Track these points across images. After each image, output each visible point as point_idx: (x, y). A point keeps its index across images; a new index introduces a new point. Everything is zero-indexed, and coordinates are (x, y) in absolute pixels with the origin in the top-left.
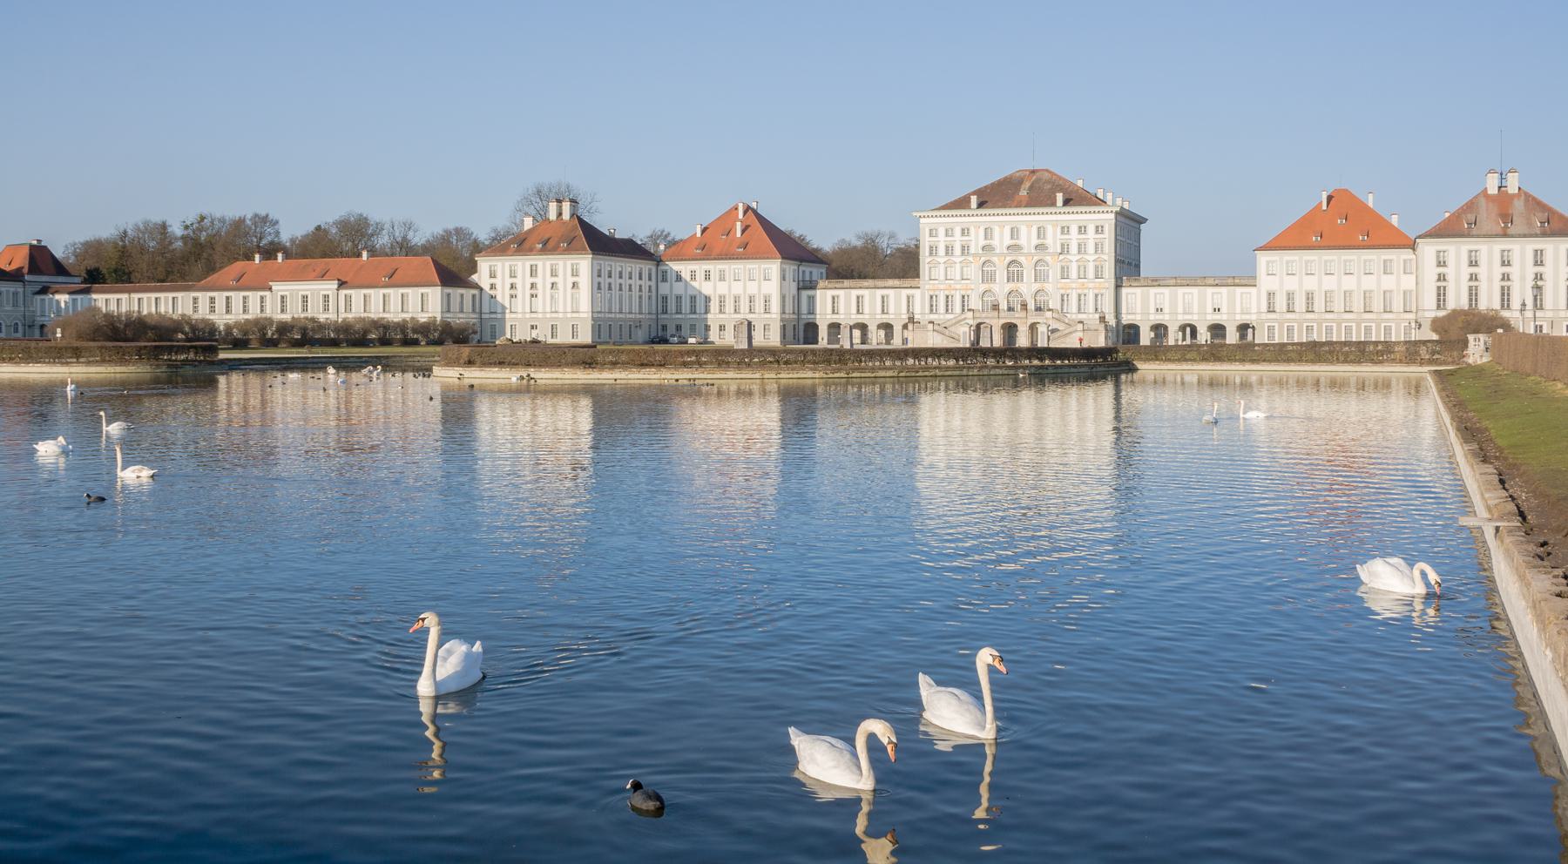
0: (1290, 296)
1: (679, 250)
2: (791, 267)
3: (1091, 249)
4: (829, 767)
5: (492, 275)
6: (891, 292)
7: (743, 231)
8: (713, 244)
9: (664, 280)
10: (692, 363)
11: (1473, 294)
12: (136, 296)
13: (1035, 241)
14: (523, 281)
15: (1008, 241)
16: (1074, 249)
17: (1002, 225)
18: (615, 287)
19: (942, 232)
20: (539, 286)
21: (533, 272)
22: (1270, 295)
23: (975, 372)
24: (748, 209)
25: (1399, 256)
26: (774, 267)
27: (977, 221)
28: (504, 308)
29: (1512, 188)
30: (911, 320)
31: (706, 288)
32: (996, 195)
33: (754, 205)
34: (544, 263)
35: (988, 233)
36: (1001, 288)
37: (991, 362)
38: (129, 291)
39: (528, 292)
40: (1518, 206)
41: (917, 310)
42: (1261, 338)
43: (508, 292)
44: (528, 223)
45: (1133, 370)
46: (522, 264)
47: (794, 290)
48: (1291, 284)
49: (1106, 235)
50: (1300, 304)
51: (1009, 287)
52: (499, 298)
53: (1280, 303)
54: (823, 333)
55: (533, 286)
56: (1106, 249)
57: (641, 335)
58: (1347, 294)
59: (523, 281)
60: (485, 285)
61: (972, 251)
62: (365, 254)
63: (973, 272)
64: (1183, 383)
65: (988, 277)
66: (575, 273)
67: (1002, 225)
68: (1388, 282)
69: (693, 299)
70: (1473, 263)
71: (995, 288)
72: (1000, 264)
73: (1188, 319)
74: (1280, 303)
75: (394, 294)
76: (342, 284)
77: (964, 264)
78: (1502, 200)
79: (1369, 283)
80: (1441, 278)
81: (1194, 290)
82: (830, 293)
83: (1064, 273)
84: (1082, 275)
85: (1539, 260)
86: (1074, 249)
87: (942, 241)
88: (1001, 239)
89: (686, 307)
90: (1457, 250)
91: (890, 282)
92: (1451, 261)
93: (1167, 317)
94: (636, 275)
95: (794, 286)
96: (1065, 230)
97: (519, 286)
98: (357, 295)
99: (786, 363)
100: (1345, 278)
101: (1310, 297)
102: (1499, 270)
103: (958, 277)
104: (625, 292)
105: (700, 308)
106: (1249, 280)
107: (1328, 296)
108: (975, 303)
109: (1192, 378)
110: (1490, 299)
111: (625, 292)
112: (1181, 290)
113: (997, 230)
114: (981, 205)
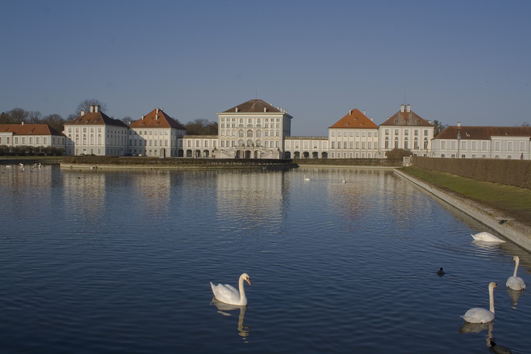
0: (339, 143)
1: (136, 124)
2: (175, 131)
3: (275, 126)
4: (477, 317)
5: (70, 132)
6: (208, 140)
7: (158, 118)
8: (148, 122)
9: (131, 134)
10: (154, 163)
11: (396, 144)
13: (257, 124)
14: (81, 134)
15: (248, 123)
16: (269, 126)
17: (246, 118)
18: (114, 136)
19: (226, 119)
20: (87, 136)
21: (85, 131)
22: (333, 143)
23: (249, 167)
24: (159, 110)
26: (168, 131)
27: (238, 116)
28: (74, 143)
29: (408, 111)
30: (215, 149)
31: (145, 137)
32: (244, 108)
33: (162, 109)
34: (89, 128)
35: (241, 120)
36: (245, 139)
37: (253, 164)
39: (83, 138)
40: (410, 116)
41: (217, 146)
42: (330, 157)
43: (75, 138)
44: (83, 113)
45: (298, 167)
46: (81, 128)
47: (175, 139)
48: (339, 139)
49: (280, 122)
50: (342, 146)
51: (248, 139)
52: (72, 140)
53: (336, 146)
54: (185, 153)
55: (84, 135)
56: (280, 126)
57: (122, 153)
58: (357, 143)
59: (81, 134)
60: (67, 135)
62: (23, 123)
63: (236, 133)
64: (313, 171)
65: (241, 135)
66: (100, 131)
67: (246, 118)
68: (370, 139)
69: (141, 141)
70: (397, 134)
71: (243, 139)
72: (245, 131)
73: (306, 150)
74: (336, 146)
75: (34, 137)
76: (14, 134)
78: (405, 114)
79: (364, 139)
80: (387, 138)
81: (308, 141)
82: (188, 140)
84: (272, 135)
86: (269, 126)
87: (226, 122)
88: (246, 123)
89: (138, 144)
90: (392, 130)
91: (208, 136)
92: (390, 133)
93: (299, 149)
94: (121, 132)
95: (175, 137)
96: (267, 120)
97: (79, 135)
98: (20, 138)
99: (186, 163)
100: (356, 138)
101: (345, 143)
102: (404, 136)
103: (231, 135)
104: (117, 138)
105: (143, 144)
106: (326, 138)
107: (351, 143)
108: (236, 144)
109: (316, 170)
110: (401, 145)
111: (117, 138)
112: (304, 141)
113: (244, 119)
114: (239, 111)
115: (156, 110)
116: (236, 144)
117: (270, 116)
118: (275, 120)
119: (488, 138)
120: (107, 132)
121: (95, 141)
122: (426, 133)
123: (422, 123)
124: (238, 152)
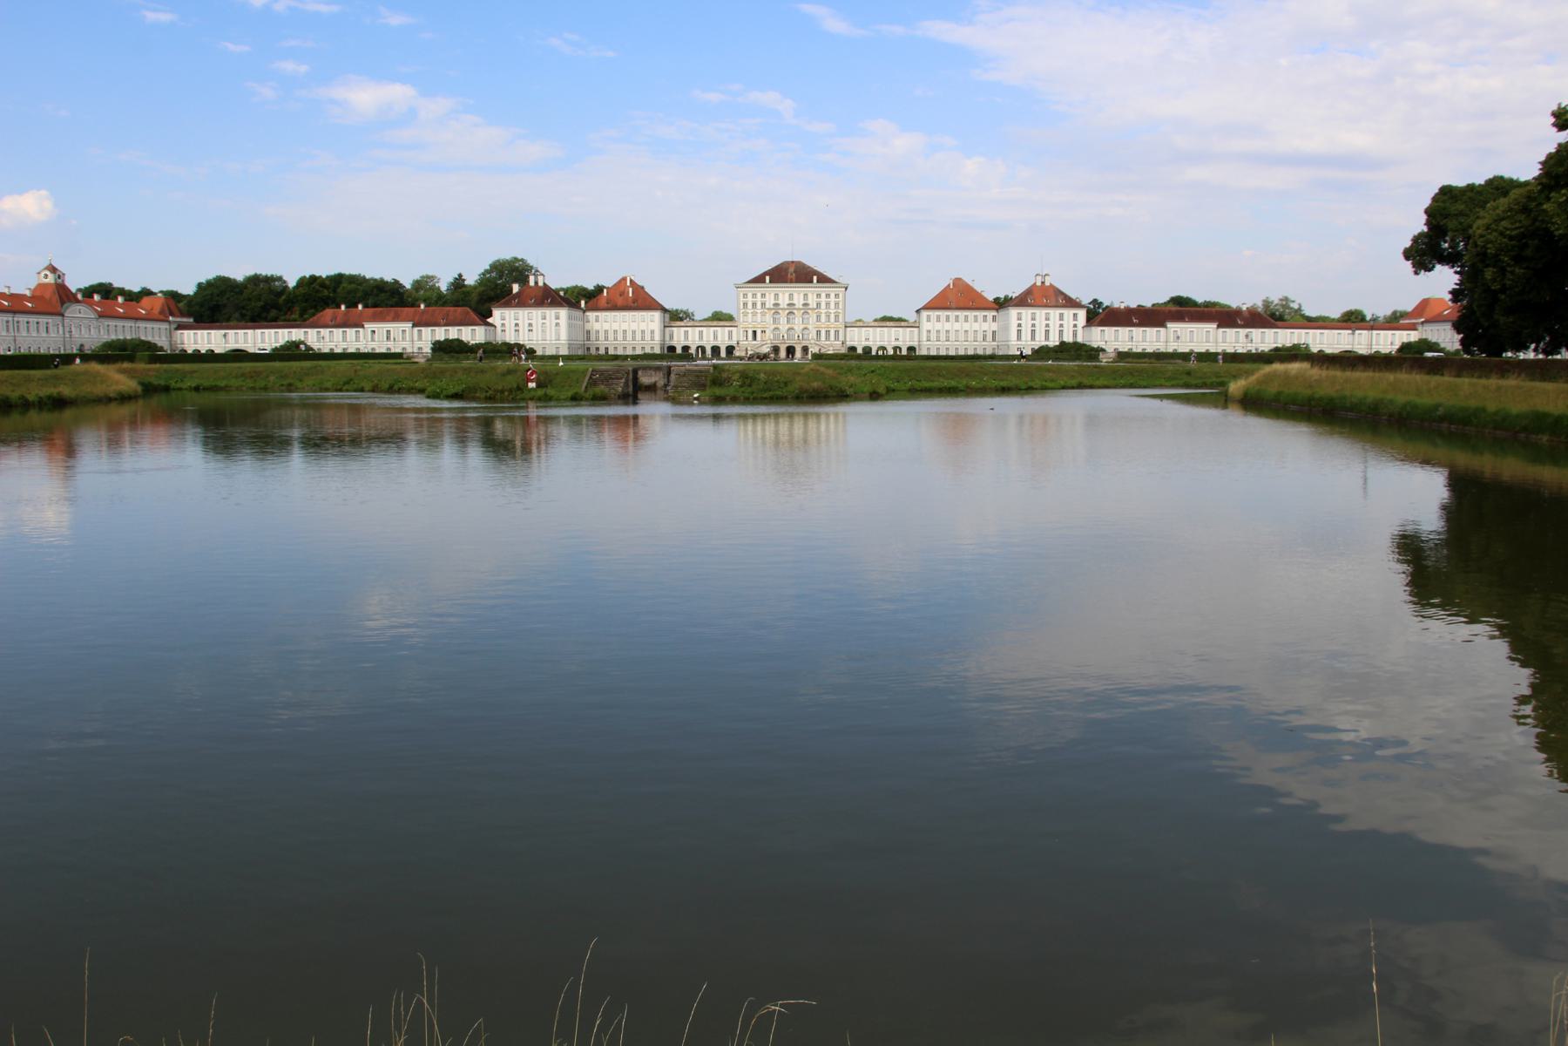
5: (503, 319)
26: (657, 315)
32: (781, 274)
34: (536, 313)
36: (784, 327)
44: (516, 288)
68: (985, 326)
72: (783, 314)
76: (414, 325)
77: (763, 314)
83: (818, 317)
85: (1061, 318)
87: (750, 299)
90: (1026, 313)
96: (819, 296)
116: (769, 335)
117: (824, 290)
120: (570, 318)
121: (551, 336)
123: (1071, 303)
124: (776, 349)
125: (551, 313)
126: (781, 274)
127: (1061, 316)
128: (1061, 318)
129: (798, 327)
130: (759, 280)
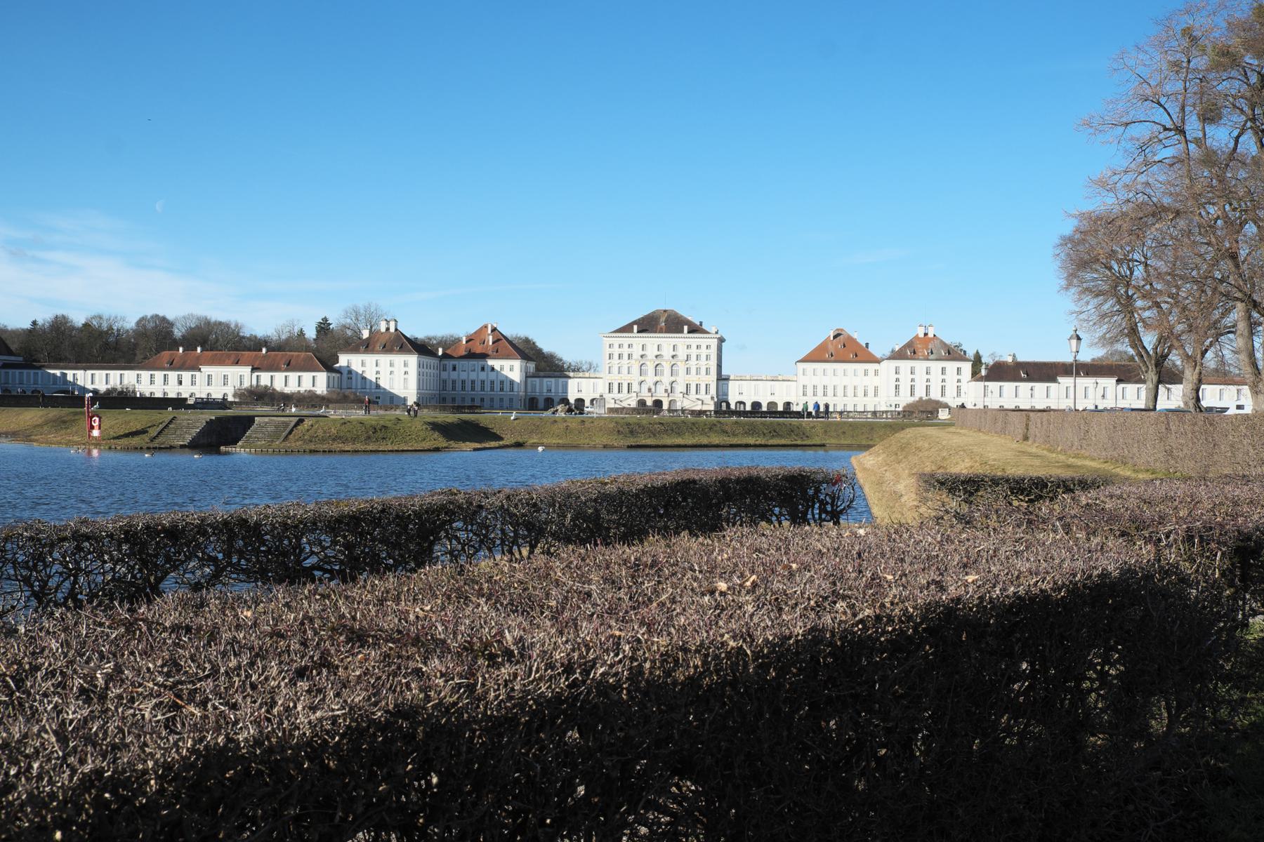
3: (703, 357)
12: (89, 372)
16: (694, 357)
24: (494, 330)
25: (871, 367)
27: (637, 341)
29: (931, 335)
36: (650, 379)
38: (85, 369)
61: (635, 357)
63: (635, 370)
75: (294, 376)
76: (254, 370)
85: (943, 370)
86: (694, 357)
88: (651, 352)
90: (905, 365)
96: (689, 347)
108: (635, 387)
114: (639, 332)
115: (486, 327)
117: (695, 340)
118: (704, 347)
119: (1054, 380)
122: (959, 370)
123: (953, 354)
124: (642, 403)
125: (398, 359)
126: (647, 325)
127: (943, 370)
128: (943, 370)
129: (666, 379)
130: (627, 329)
